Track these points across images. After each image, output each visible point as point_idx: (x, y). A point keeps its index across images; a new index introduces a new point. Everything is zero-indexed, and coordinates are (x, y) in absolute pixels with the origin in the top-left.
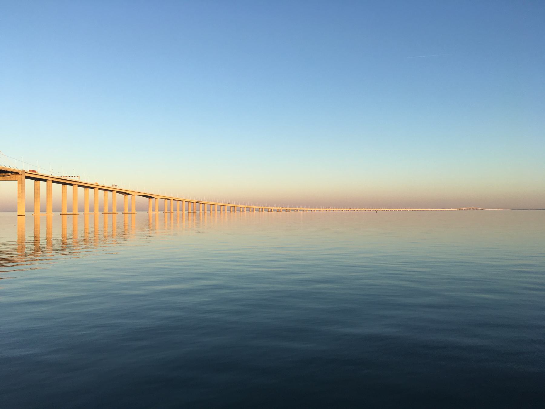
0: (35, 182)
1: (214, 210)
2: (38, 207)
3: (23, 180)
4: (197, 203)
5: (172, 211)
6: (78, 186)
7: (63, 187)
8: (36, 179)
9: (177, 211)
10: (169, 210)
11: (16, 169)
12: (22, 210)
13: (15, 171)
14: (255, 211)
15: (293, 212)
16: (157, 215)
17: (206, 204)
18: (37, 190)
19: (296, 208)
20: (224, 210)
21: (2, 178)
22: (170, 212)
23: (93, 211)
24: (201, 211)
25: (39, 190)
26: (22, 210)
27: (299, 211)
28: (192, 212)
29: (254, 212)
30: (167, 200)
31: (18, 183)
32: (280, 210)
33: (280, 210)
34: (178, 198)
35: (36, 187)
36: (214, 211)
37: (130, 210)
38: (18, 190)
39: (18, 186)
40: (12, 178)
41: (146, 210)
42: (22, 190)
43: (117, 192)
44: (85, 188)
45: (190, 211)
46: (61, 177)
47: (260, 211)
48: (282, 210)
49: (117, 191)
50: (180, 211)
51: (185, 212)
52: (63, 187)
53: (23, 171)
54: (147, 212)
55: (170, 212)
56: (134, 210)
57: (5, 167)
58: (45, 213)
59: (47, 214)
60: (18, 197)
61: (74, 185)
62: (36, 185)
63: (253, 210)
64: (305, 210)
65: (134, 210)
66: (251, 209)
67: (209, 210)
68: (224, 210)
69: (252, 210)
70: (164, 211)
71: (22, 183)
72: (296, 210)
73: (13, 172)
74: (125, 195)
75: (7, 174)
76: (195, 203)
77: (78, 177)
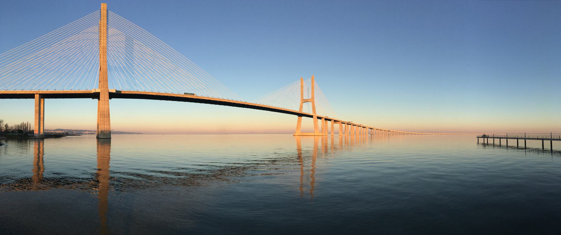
1: (394, 134)
32: (419, 134)
33: (419, 134)
34: (381, 129)
43: (363, 127)
56: (367, 134)
65: (367, 134)
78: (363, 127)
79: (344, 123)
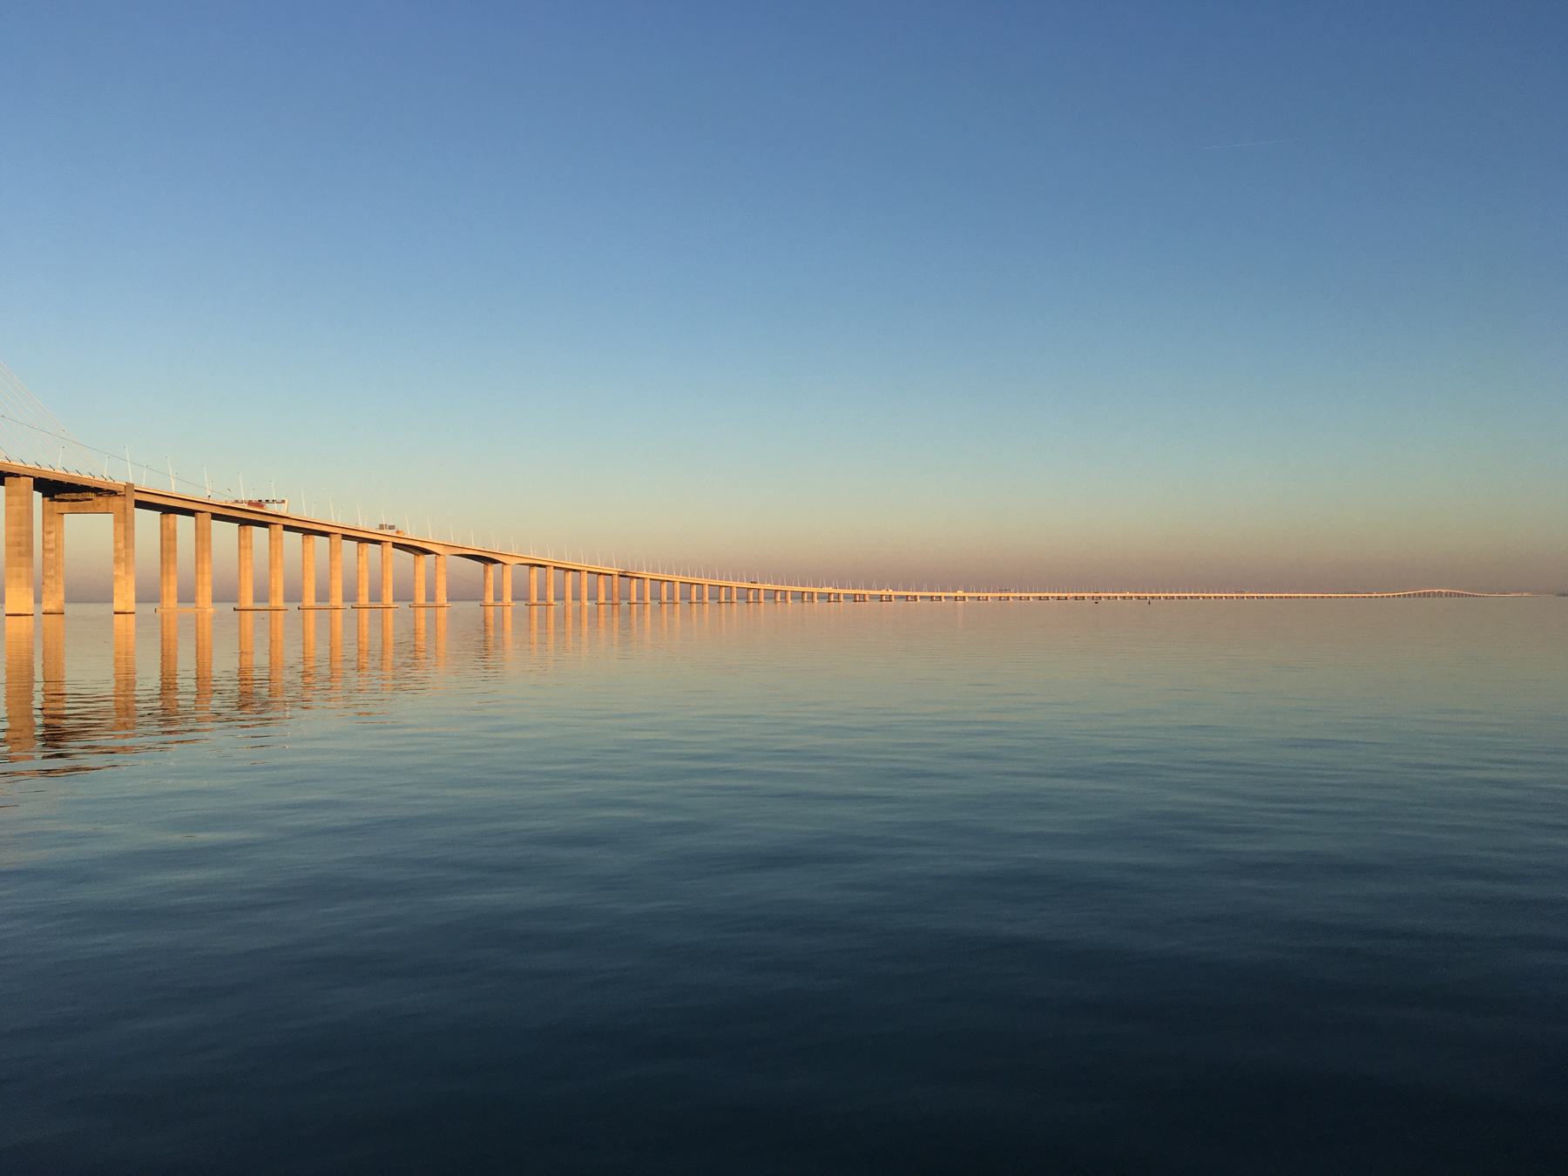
0: (161, 519)
1: (671, 597)
2: (171, 589)
3: (128, 511)
4: (621, 576)
5: (552, 601)
6: (284, 530)
7: (242, 531)
8: (167, 510)
9: (564, 599)
10: (542, 597)
11: (109, 481)
12: (124, 598)
13: (106, 488)
14: (790, 601)
15: (903, 602)
16: (508, 612)
17: (648, 580)
18: (168, 541)
19: (909, 591)
20: (700, 597)
21: (70, 507)
22: (544, 602)
23: (267, 601)
24: (634, 599)
25: (175, 540)
26: (124, 598)
27: (919, 600)
28: (606, 602)
29: (786, 602)
30: (536, 568)
31: (116, 521)
35: (165, 532)
36: (671, 601)
37: (431, 596)
38: (116, 542)
39: (115, 529)
40: (99, 505)
41: (479, 597)
42: (126, 538)
43: (396, 545)
44: (304, 534)
45: (602, 599)
46: (237, 502)
47: (806, 599)
48: (870, 598)
49: (393, 543)
50: (573, 599)
51: (587, 604)
52: (242, 531)
53: (129, 486)
54: (478, 603)
55: (544, 602)
56: (442, 598)
57: (78, 475)
58: (194, 605)
59: (197, 608)
60: (117, 560)
61: (273, 526)
62: (164, 527)
63: (784, 598)
64: (937, 597)
65: (442, 598)
66: (779, 594)
67: (656, 596)
68: (700, 597)
69: (781, 598)
70: (528, 599)
71: (125, 521)
72: (909, 598)
73: (101, 490)
74: (418, 555)
75: (84, 494)
76: (616, 578)
77: (283, 502)
78: (396, 545)
79: (191, 513)
